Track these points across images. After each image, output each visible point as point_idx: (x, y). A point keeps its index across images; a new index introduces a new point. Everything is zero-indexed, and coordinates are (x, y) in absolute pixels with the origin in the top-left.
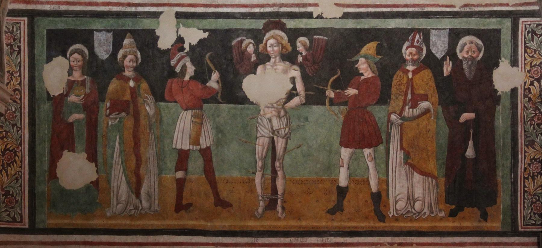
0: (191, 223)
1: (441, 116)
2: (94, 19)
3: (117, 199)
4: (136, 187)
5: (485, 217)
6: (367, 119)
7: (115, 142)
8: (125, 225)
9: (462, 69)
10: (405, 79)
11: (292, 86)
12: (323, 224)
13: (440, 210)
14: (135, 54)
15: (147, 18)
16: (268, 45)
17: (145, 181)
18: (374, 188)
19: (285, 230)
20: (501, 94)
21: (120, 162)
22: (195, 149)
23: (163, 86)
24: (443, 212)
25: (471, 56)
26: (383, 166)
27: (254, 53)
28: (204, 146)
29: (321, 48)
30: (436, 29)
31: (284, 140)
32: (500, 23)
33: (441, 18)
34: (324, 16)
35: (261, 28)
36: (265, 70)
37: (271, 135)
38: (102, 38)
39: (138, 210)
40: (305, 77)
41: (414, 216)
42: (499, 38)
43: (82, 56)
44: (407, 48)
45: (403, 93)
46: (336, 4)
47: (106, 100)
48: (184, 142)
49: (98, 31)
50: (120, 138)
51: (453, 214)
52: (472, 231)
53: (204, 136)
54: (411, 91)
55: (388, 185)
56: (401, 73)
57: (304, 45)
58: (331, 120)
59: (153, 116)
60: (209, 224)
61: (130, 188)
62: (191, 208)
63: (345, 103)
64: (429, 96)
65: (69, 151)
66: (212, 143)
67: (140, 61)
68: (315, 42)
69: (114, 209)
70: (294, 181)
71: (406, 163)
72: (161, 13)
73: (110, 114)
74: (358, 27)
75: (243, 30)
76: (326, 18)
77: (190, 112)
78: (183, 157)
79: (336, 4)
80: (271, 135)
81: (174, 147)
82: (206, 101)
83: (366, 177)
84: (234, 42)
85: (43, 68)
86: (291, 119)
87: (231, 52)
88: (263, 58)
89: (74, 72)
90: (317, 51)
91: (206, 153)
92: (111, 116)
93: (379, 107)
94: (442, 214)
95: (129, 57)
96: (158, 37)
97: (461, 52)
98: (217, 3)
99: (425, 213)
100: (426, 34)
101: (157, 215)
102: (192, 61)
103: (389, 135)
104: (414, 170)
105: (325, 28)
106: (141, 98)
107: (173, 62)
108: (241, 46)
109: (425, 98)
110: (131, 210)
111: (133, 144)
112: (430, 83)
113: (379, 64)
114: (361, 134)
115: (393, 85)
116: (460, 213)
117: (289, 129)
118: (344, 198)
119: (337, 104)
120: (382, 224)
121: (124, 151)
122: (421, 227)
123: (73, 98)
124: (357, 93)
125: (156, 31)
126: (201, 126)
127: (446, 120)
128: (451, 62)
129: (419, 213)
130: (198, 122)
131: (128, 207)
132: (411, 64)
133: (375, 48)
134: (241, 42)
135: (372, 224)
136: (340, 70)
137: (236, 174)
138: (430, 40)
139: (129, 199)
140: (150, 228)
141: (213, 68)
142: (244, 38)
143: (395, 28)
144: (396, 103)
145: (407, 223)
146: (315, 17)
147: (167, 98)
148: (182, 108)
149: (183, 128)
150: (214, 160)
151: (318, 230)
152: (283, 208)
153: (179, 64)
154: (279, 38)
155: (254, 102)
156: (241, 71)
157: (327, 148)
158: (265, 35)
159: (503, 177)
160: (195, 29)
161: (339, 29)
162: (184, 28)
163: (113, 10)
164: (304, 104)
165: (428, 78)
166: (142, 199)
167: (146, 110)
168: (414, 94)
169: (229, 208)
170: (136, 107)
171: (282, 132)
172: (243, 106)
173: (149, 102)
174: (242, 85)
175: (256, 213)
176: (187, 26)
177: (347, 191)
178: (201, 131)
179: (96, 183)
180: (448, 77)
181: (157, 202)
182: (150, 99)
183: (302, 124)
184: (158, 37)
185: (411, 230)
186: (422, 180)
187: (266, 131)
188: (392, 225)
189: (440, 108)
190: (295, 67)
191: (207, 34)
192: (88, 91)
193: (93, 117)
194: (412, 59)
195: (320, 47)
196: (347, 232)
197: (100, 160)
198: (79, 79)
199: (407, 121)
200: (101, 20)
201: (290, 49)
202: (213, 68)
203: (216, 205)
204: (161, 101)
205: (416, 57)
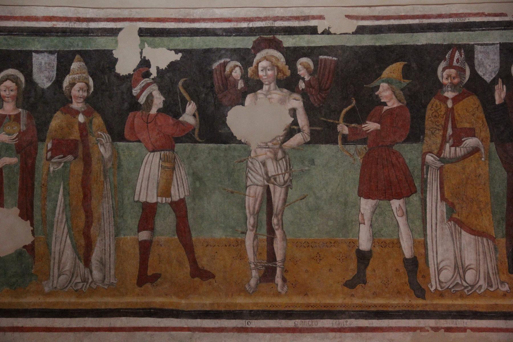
0: (158, 301)
1: (496, 156)
2: (32, 37)
3: (59, 269)
4: (85, 253)
7: (58, 193)
8: (69, 303)
10: (443, 109)
11: (293, 119)
12: (339, 301)
13: (502, 283)
14: (86, 81)
15: (101, 36)
16: (260, 69)
17: (98, 245)
18: (408, 253)
19: (286, 309)
21: (64, 220)
22: (164, 202)
24: (507, 286)
26: (418, 223)
27: (241, 78)
28: (176, 198)
29: (329, 73)
30: (482, 45)
31: (283, 190)
33: (488, 30)
34: (332, 31)
35: (250, 47)
36: (257, 99)
37: (266, 183)
38: (43, 62)
39: (87, 282)
40: (308, 108)
41: (466, 291)
43: (17, 84)
44: (444, 69)
45: (440, 127)
46: (347, 16)
47: (47, 140)
48: (149, 192)
49: (37, 52)
50: (64, 188)
53: (176, 185)
54: (452, 124)
56: (437, 102)
57: (307, 68)
58: (346, 163)
59: (109, 160)
60: (183, 302)
61: (78, 254)
62: (159, 280)
63: (364, 141)
64: (477, 131)
66: (186, 194)
67: (92, 90)
68: (321, 64)
69: (55, 282)
70: (297, 244)
71: (450, 219)
72: (120, 29)
73: (52, 157)
74: (378, 44)
75: (226, 50)
76: (335, 34)
77: (157, 155)
78: (148, 214)
79: (347, 16)
80: (266, 183)
81: (136, 199)
82: (178, 140)
83: (395, 237)
84: (215, 66)
86: (292, 163)
87: (212, 78)
88: (254, 85)
90: (324, 75)
91: (179, 208)
92: (53, 160)
95: (78, 85)
96: (116, 60)
98: (192, 17)
99: (481, 286)
100: (469, 51)
101: (114, 290)
102: (161, 90)
103: (424, 182)
104: (461, 227)
105: (334, 47)
106: (93, 136)
107: (135, 91)
108: (224, 71)
109: (471, 133)
110: (76, 283)
111: (82, 196)
113: (407, 89)
114: (387, 180)
115: (427, 117)
117: (290, 175)
118: (367, 266)
119: (353, 142)
120: (420, 302)
121: (70, 205)
122: (477, 306)
124: (379, 128)
125: (114, 52)
126: (173, 173)
127: (502, 161)
128: (504, 86)
129: (473, 286)
130: (169, 168)
131: (74, 279)
132: (449, 89)
133: (401, 70)
134: (225, 65)
135: (407, 301)
136: (356, 99)
137: (219, 234)
138: (474, 58)
139: (75, 267)
140: (103, 307)
141: (188, 98)
142: (228, 60)
143: (426, 45)
144: (432, 140)
146: (319, 32)
147: (127, 137)
148: (147, 148)
149: (148, 176)
150: (190, 215)
151: (331, 309)
152: (284, 280)
153: (144, 94)
154: (274, 60)
155: (243, 141)
156: (225, 101)
157: (342, 200)
158: (255, 56)
160: (165, 50)
161: (351, 47)
162: (150, 48)
163: (58, 26)
164: (308, 143)
165: (474, 107)
166: (93, 268)
167: (100, 152)
168: (456, 127)
169: (211, 280)
170: (86, 147)
171: (281, 179)
172: (227, 145)
173: (104, 142)
174: (226, 119)
175: (247, 286)
176: (154, 46)
177: (371, 256)
178: (172, 179)
179: (30, 248)
180: (501, 105)
181: (112, 272)
182: (106, 137)
183: (307, 168)
184: (116, 60)
185: (463, 309)
186: (473, 243)
187: (258, 177)
188: (435, 302)
189: (493, 146)
190: (296, 96)
191: (180, 55)
192: (23, 128)
193: (30, 161)
194: (450, 83)
195: (327, 71)
196: (373, 312)
197: (37, 217)
198: (11, 114)
199: (448, 162)
200: (42, 39)
201: (288, 73)
202: (188, 98)
203: (193, 276)
204: (120, 141)
205: (456, 81)
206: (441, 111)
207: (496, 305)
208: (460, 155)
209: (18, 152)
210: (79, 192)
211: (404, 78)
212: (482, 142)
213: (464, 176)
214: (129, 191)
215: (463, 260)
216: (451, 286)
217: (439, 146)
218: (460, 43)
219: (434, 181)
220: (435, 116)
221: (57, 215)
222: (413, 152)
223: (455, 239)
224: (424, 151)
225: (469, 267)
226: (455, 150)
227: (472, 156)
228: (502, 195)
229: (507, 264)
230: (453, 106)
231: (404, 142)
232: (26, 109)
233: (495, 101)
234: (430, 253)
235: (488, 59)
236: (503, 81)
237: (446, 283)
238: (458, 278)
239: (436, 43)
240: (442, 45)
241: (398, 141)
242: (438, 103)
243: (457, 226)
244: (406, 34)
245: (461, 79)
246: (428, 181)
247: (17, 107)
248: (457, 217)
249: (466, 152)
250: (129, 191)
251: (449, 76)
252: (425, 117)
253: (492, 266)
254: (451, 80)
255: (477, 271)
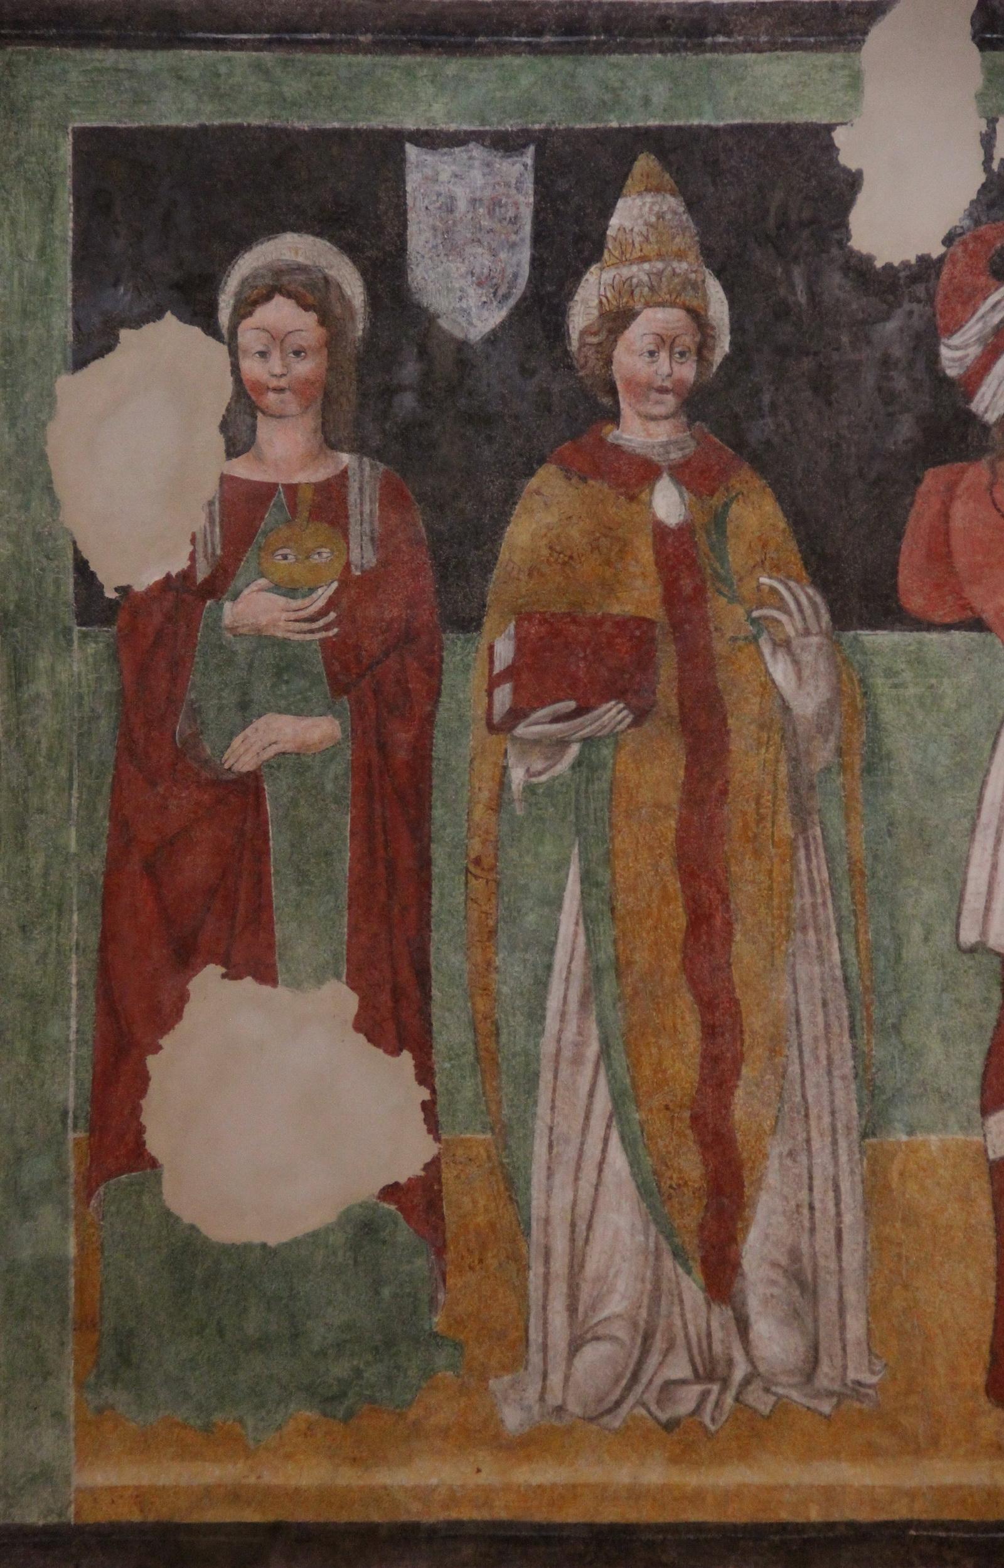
3: (572, 1309)
7: (557, 904)
8: (635, 1494)
14: (689, 298)
17: (772, 1178)
21: (593, 1049)
23: (889, 525)
38: (462, 194)
39: (725, 1382)
43: (324, 319)
47: (489, 622)
49: (430, 140)
50: (587, 878)
59: (822, 729)
61: (668, 1232)
65: (233, 974)
67: (723, 345)
69: (556, 1378)
73: (516, 715)
81: (969, 935)
85: (48, 398)
89: (265, 429)
92: (521, 730)
95: (650, 322)
96: (854, 181)
106: (734, 599)
110: (669, 1385)
111: (680, 921)
121: (621, 967)
123: (257, 606)
147: (914, 602)
167: (769, 686)
170: (696, 659)
173: (790, 628)
182: (799, 605)
184: (854, 181)
192: (363, 556)
193: (402, 736)
197: (450, 1029)
198: (300, 478)
204: (874, 625)
209: (338, 687)
210: (666, 898)
214: (930, 896)
221: (551, 1023)
232: (378, 454)
247: (331, 444)
250: (930, 896)
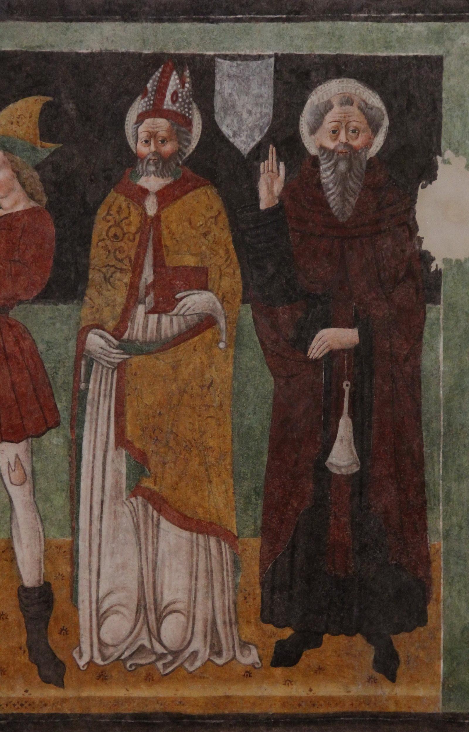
5: (388, 666)
6: (10, 347)
9: (319, 185)
10: (135, 219)
13: (245, 645)
20: (441, 266)
24: (254, 652)
25: (346, 145)
26: (60, 500)
30: (232, 58)
32: (438, 38)
33: (250, 20)
41: (160, 665)
42: (438, 84)
44: (141, 118)
51: (285, 657)
52: (346, 714)
54: (155, 257)
55: (74, 563)
64: (213, 275)
71: (135, 490)
93: (48, 307)
94: (251, 657)
97: (313, 131)
99: (195, 654)
100: (202, 73)
103: (79, 399)
104: (159, 511)
112: (216, 231)
113: (50, 167)
115: (95, 238)
116: (307, 652)
120: (52, 692)
122: (182, 702)
127: (265, 350)
128: (282, 165)
129: (176, 654)
132: (152, 168)
133: (36, 118)
138: (213, 91)
143: (100, 54)
144: (104, 296)
145: (136, 685)
159: (447, 536)
165: (208, 215)
168: (163, 265)
180: (272, 211)
185: (149, 709)
188: (85, 694)
189: (247, 313)
194: (155, 153)
199: (140, 352)
205: (168, 148)
206: (130, 224)
207: (228, 697)
208: (169, 335)
211: (43, 137)
212: (222, 304)
213: (174, 387)
215: (159, 589)
216: (127, 654)
217: (119, 310)
218: (181, 52)
219: (102, 398)
220: (115, 235)
222: (58, 325)
223: (143, 540)
224: (83, 324)
225: (172, 607)
226: (159, 321)
227: (197, 338)
228: (258, 432)
229: (259, 599)
230: (159, 211)
231: (38, 299)
233: (257, 199)
234: (83, 575)
235: (247, 94)
236: (278, 153)
237: (114, 646)
238: (144, 634)
239: (123, 50)
240: (140, 54)
241: (24, 297)
242: (124, 205)
243: (150, 508)
244: (50, 24)
245: (179, 143)
246: (90, 396)
248: (152, 486)
249: (183, 326)
251: (152, 135)
252: (90, 237)
253: (224, 603)
254: (156, 147)
255: (188, 619)
